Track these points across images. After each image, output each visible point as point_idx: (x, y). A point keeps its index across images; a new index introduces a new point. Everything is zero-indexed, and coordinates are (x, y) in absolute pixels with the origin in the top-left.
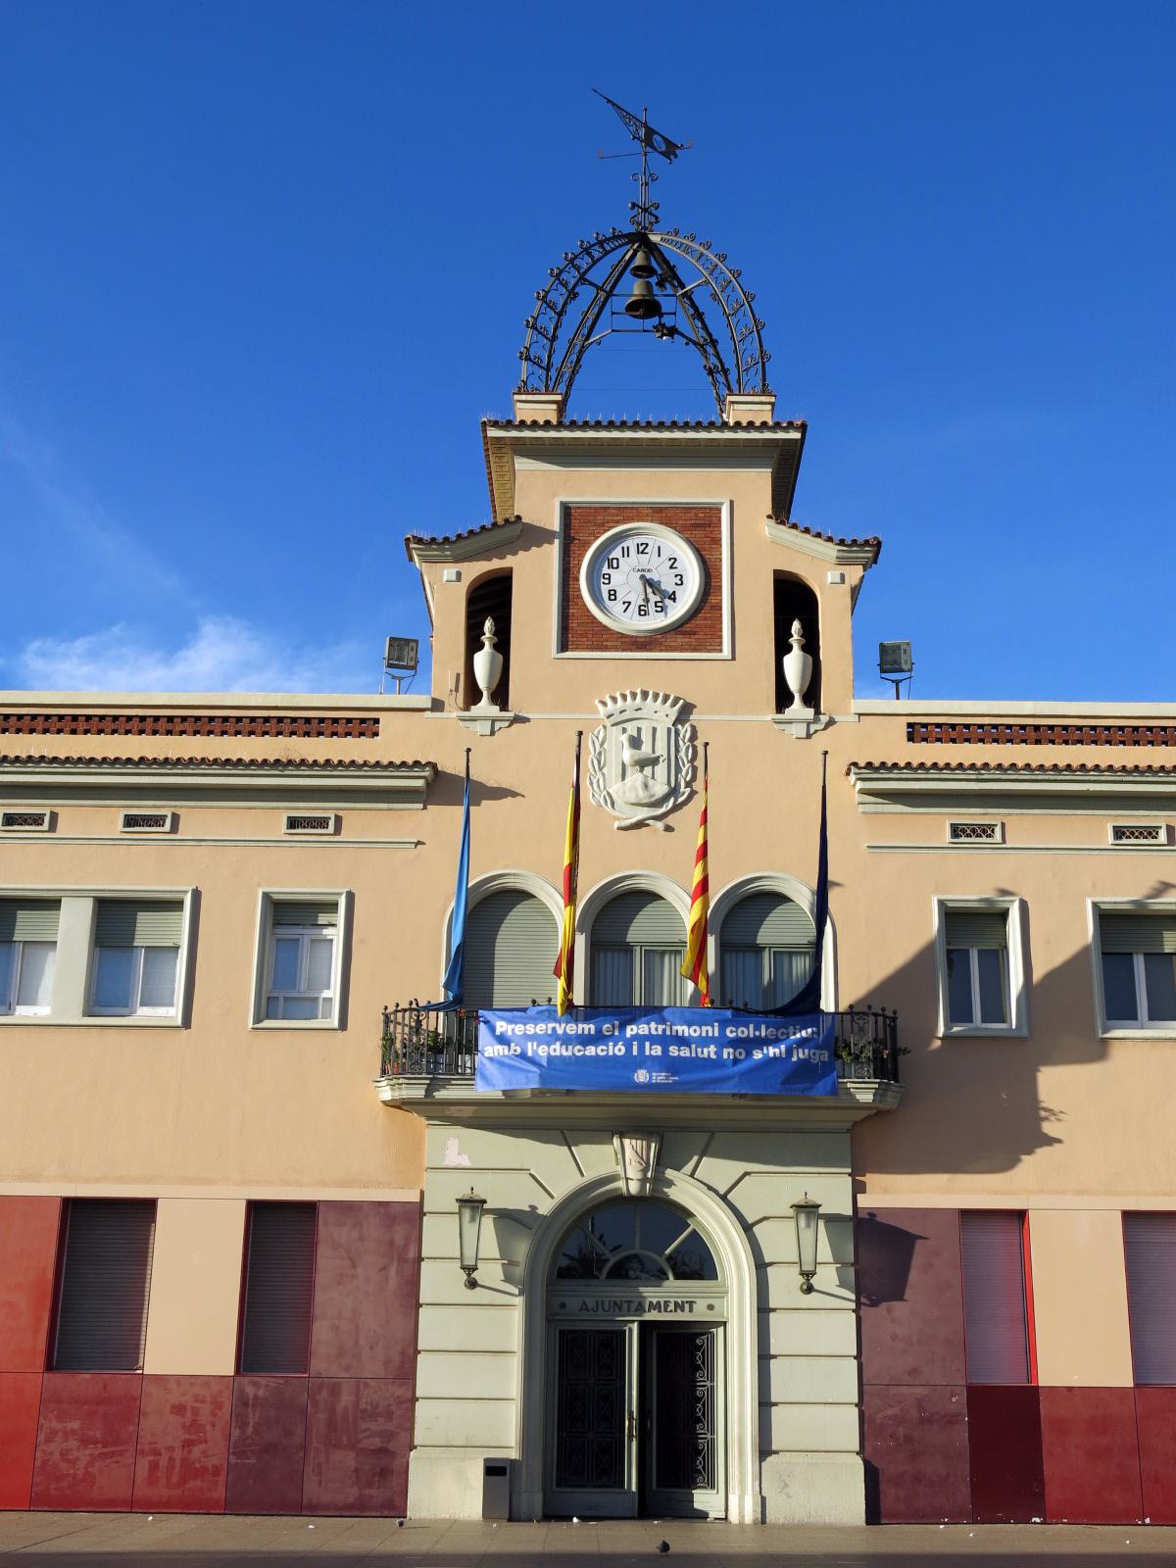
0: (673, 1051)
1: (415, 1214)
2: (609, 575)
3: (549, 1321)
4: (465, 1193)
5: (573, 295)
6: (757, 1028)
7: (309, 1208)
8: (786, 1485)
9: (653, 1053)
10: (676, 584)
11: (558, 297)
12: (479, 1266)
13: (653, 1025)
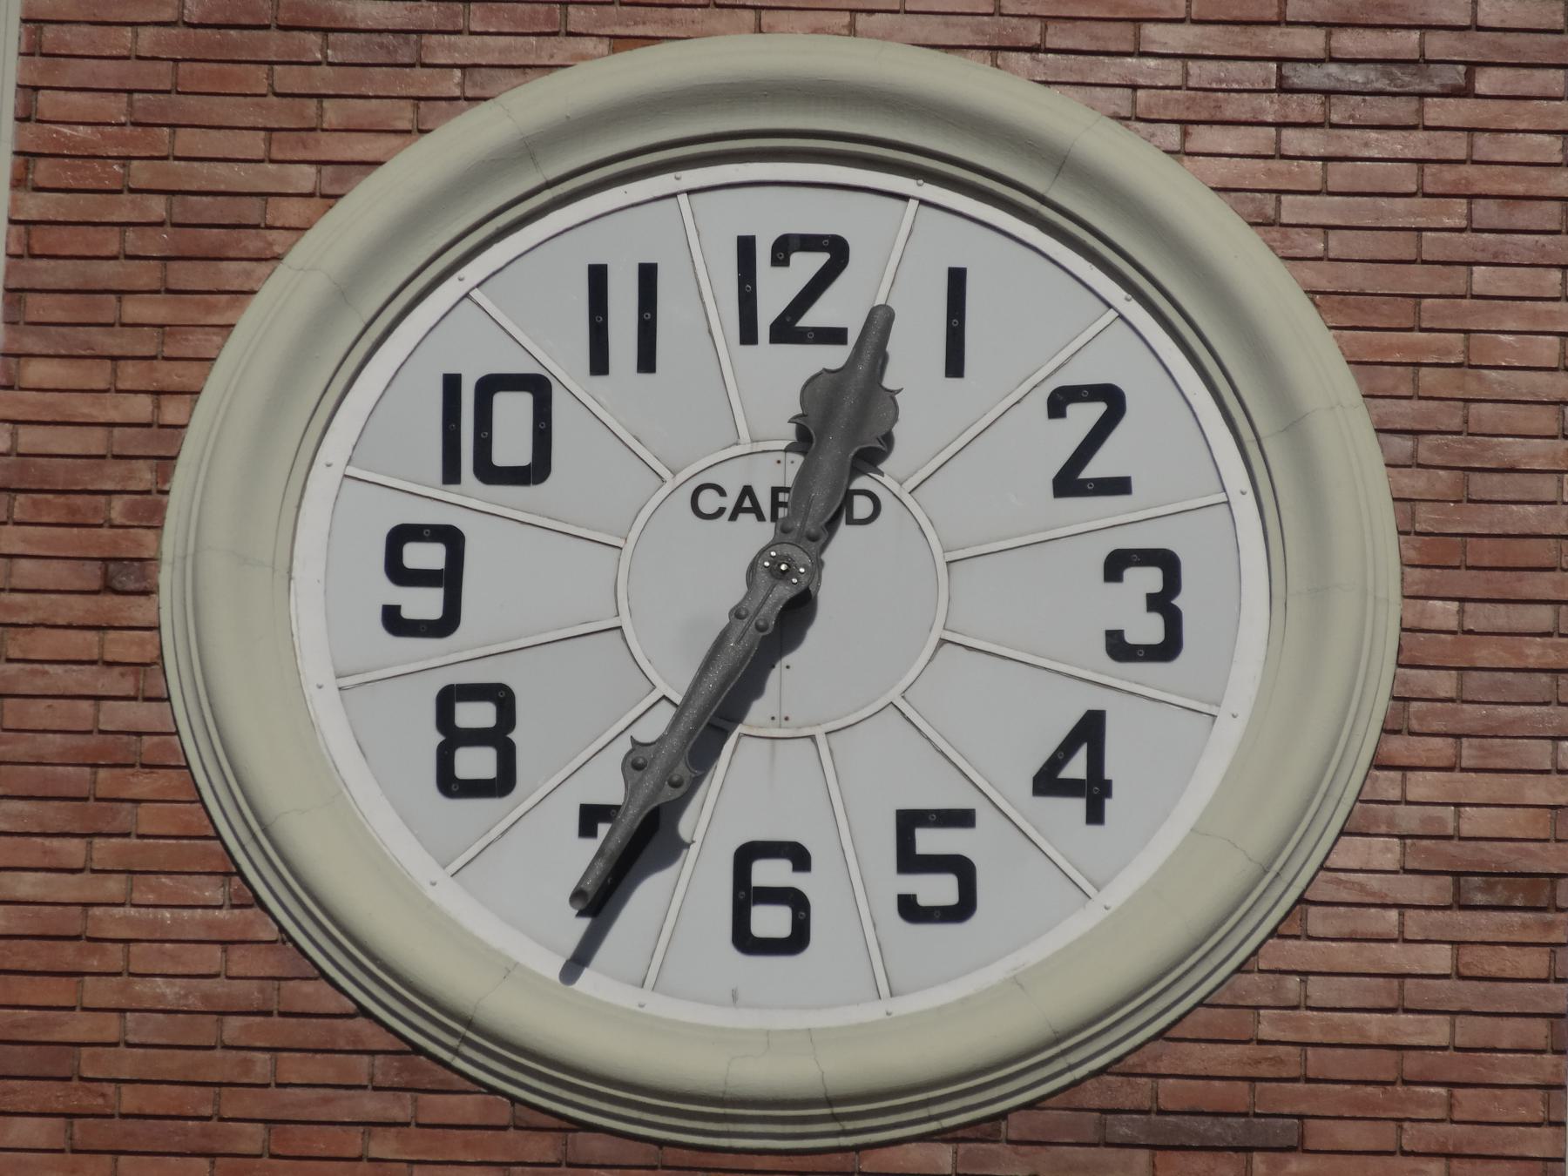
2: (451, 538)
10: (1119, 647)
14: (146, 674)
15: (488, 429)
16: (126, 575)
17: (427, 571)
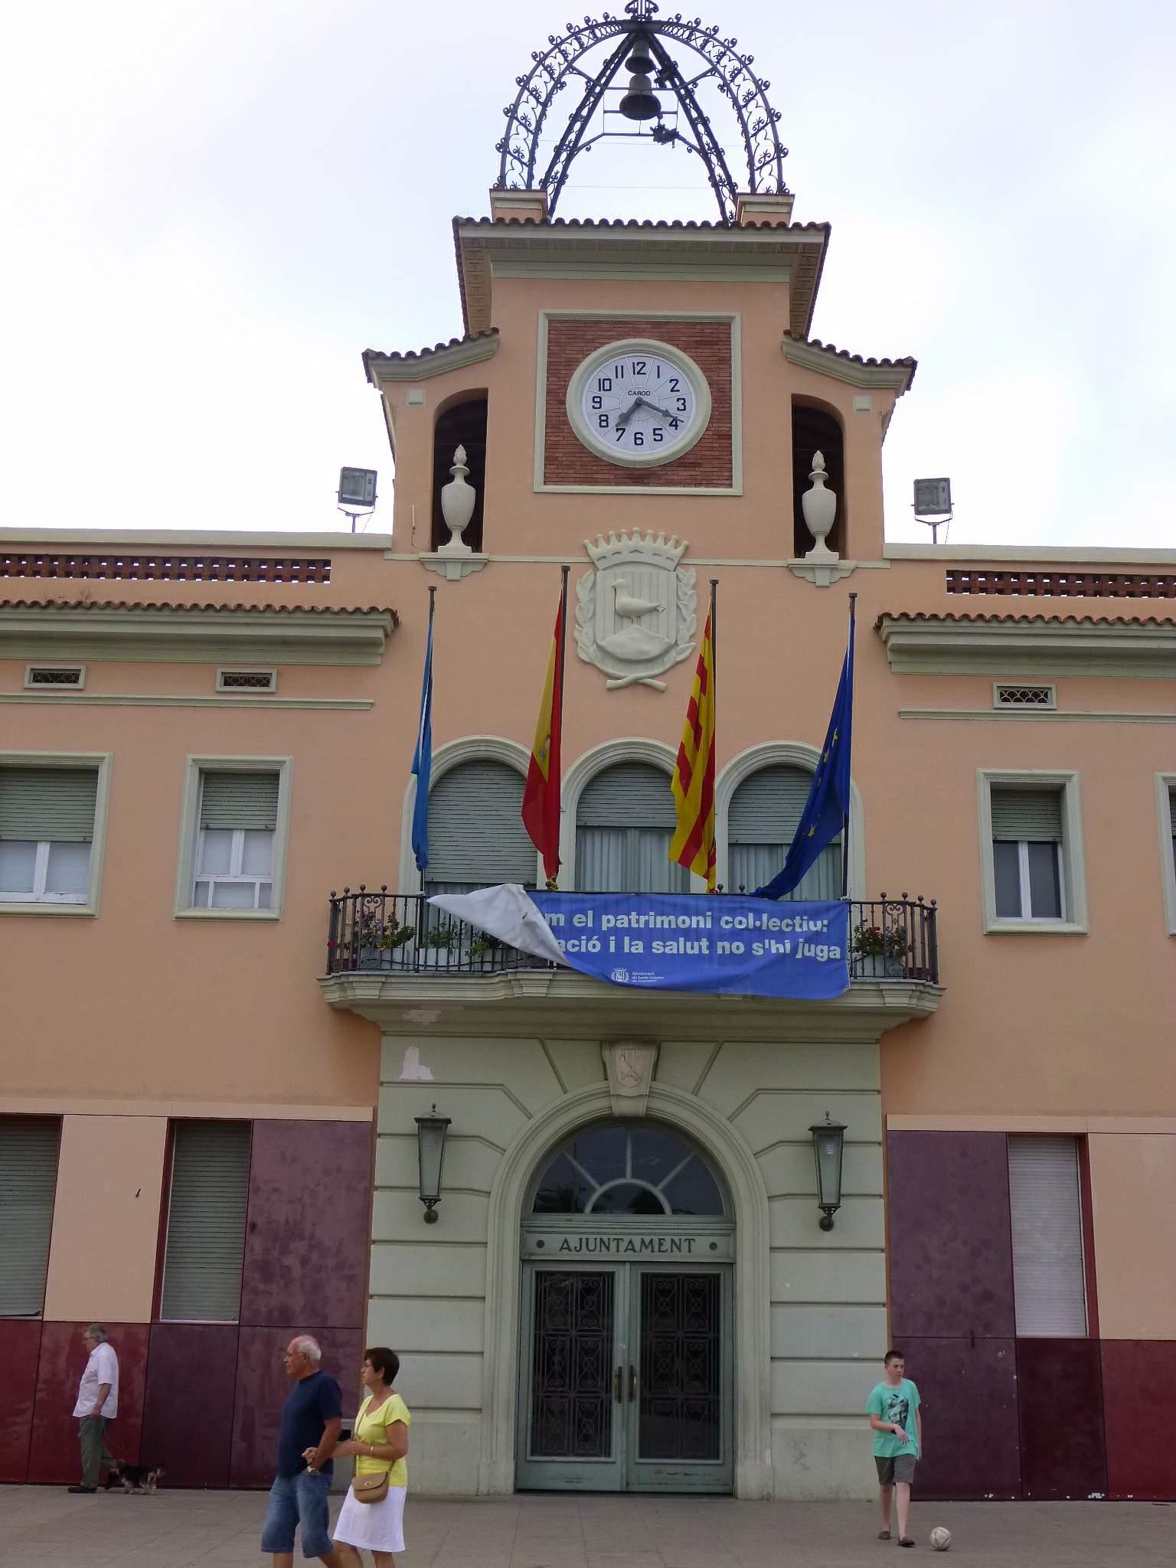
0: (658, 947)
1: (365, 1135)
3: (524, 1262)
4: (426, 1112)
5: (559, 85)
6: (758, 917)
7: (242, 1128)
8: (803, 1455)
9: (633, 950)
11: (541, 83)
12: (442, 1196)
13: (634, 916)
14: (565, 414)
15: (604, 385)
16: (563, 402)
17: (597, 401)
